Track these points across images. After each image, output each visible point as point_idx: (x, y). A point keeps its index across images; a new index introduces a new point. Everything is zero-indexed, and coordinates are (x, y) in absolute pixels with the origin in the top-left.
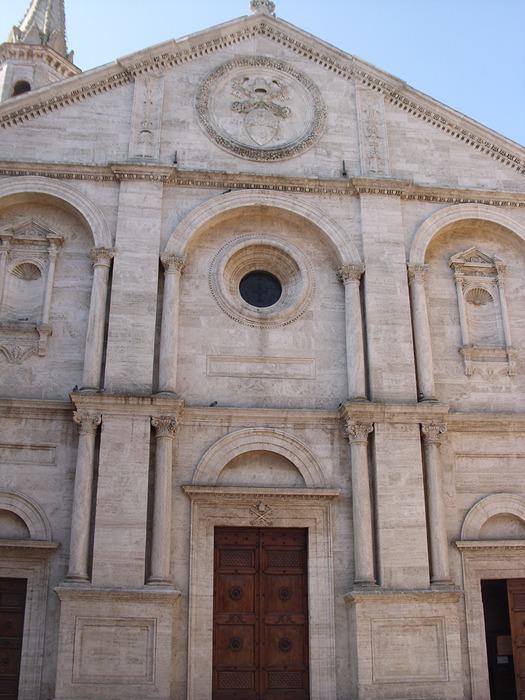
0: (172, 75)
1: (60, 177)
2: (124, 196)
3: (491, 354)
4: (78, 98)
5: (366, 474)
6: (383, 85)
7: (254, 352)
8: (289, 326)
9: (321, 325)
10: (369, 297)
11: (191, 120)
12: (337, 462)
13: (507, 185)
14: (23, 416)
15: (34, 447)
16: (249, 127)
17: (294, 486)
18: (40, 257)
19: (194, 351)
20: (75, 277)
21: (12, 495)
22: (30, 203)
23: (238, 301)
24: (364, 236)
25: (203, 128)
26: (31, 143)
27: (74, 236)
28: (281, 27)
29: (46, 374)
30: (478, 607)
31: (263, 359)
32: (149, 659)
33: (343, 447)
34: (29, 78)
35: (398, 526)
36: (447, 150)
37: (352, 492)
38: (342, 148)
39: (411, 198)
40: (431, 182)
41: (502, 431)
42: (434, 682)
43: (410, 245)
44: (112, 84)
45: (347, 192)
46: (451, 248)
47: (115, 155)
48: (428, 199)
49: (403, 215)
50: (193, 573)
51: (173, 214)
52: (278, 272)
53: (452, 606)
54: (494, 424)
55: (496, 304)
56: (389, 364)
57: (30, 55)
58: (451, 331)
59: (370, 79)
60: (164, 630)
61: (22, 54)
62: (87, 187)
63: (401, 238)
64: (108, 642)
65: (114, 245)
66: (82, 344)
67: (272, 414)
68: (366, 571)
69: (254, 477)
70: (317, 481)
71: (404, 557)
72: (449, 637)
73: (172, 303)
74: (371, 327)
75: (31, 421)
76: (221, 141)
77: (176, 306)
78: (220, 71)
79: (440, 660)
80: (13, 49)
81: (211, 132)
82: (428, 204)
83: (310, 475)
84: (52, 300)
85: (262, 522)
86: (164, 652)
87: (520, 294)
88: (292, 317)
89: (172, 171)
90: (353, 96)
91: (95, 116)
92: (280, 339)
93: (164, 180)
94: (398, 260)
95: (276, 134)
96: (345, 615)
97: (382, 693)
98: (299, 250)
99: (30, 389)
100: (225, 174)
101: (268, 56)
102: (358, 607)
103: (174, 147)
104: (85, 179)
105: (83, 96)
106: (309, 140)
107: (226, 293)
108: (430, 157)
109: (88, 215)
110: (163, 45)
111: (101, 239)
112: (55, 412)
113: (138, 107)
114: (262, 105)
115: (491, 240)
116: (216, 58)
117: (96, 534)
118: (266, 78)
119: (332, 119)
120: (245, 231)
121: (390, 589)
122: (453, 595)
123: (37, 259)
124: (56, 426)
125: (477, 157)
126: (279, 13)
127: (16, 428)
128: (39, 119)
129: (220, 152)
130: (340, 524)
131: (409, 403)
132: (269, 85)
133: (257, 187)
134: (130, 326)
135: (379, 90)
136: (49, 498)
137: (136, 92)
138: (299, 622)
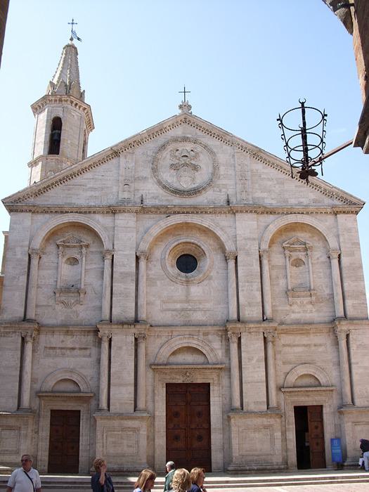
0: (139, 150)
1: (85, 213)
2: (118, 222)
3: (303, 294)
5: (237, 357)
9: (216, 283)
12: (224, 351)
13: (315, 201)
15: (81, 349)
16: (179, 177)
17: (203, 364)
21: (71, 371)
22: (71, 226)
26: (69, 194)
29: (84, 312)
30: (292, 420)
31: (188, 301)
34: (61, 115)
38: (228, 187)
39: (262, 213)
41: (307, 333)
42: (268, 455)
43: (261, 239)
45: (229, 213)
46: (284, 237)
47: (111, 200)
48: (271, 213)
51: (141, 229)
54: (302, 330)
55: (307, 266)
57: (60, 100)
59: (242, 147)
60: (143, 432)
61: (56, 101)
62: (98, 217)
63: (256, 236)
66: (101, 298)
67: (191, 329)
68: (237, 404)
70: (214, 361)
71: (255, 396)
73: (143, 276)
74: (240, 284)
76: (164, 187)
77: (145, 277)
78: (163, 147)
80: (51, 98)
81: (159, 183)
82: (271, 216)
83: (211, 358)
84: (85, 276)
85: (188, 381)
86: (143, 442)
87: (320, 261)
88: (202, 279)
90: (234, 156)
91: (100, 177)
92: (196, 290)
93: (136, 212)
97: (243, 460)
98: (206, 244)
102: (232, 421)
103: (141, 192)
106: (210, 184)
107: (170, 269)
108: (274, 188)
110: (134, 137)
111: (107, 245)
113: (122, 171)
114: (186, 165)
115: (306, 231)
116: (161, 140)
119: (222, 170)
121: (247, 412)
122: (277, 414)
124: (90, 338)
125: (300, 186)
126: (194, 111)
127: (71, 340)
128: (73, 181)
130: (225, 381)
131: (258, 322)
133: (183, 213)
138: (206, 427)
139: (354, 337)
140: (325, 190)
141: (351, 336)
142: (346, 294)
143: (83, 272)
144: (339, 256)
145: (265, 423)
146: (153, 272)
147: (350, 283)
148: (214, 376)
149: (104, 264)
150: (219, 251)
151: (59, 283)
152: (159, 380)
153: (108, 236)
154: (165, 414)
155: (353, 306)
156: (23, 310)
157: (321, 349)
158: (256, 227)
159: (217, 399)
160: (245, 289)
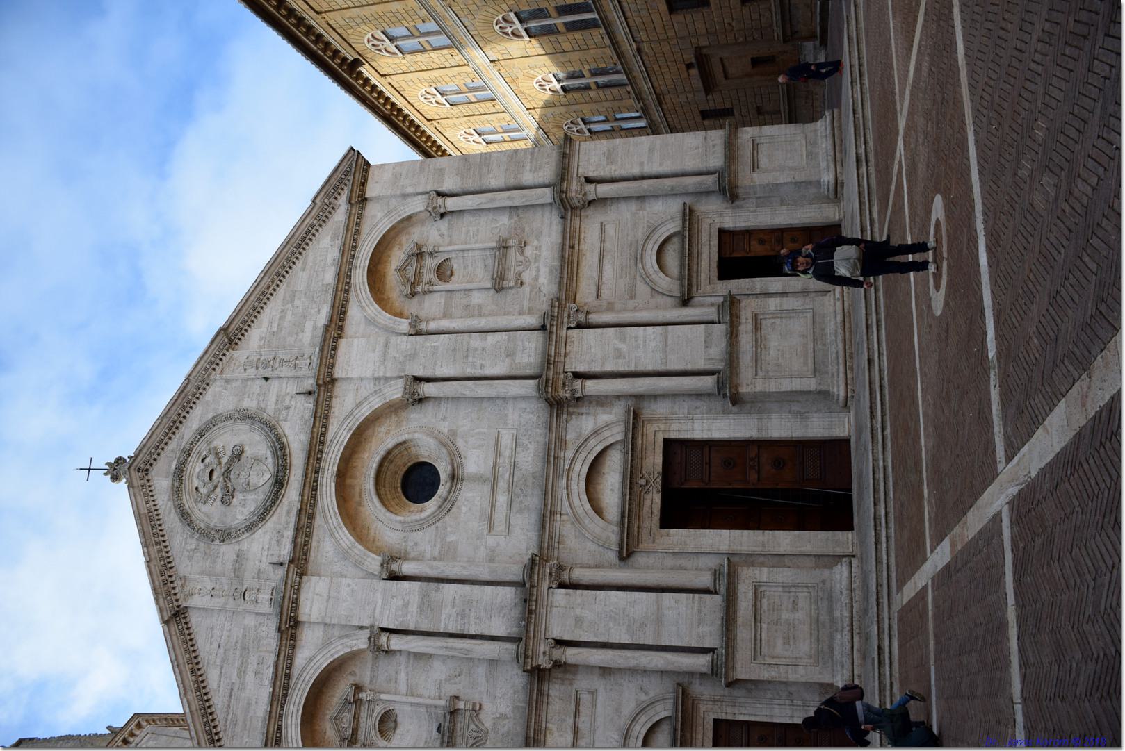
1: (287, 687)
4: (199, 669)
6: (220, 350)
7: (487, 489)
8: (462, 453)
10: (439, 373)
11: (237, 547)
12: (599, 410)
14: (543, 726)
15: (577, 714)
18: (373, 711)
19: (482, 548)
20: (396, 673)
23: (432, 505)
24: (376, 375)
25: (246, 535)
26: (245, 721)
28: (144, 451)
31: (495, 478)
32: (793, 589)
33: (587, 403)
35: (666, 352)
36: (294, 292)
37: (630, 396)
39: (341, 329)
40: (325, 310)
44: (187, 632)
45: (331, 391)
48: (344, 313)
49: (358, 337)
50: (708, 549)
52: (405, 465)
53: (742, 304)
55: (453, 255)
56: (507, 356)
58: (477, 298)
59: (212, 363)
60: (762, 574)
63: (382, 340)
64: (776, 631)
65: (366, 628)
66: (469, 660)
68: (708, 382)
69: (612, 490)
72: (772, 308)
73: (432, 567)
74: (469, 371)
75: (549, 718)
77: (435, 563)
78: (185, 516)
79: (793, 317)
81: (251, 527)
84: (419, 696)
86: (785, 575)
89: (292, 565)
90: (228, 381)
92: (475, 463)
94: (405, 343)
95: (260, 461)
96: (748, 406)
99: (514, 719)
100: (300, 511)
101: (173, 467)
103: (265, 566)
105: (197, 663)
107: (424, 515)
109: (332, 655)
111: (360, 642)
112: (540, 692)
113: (217, 603)
116: (171, 520)
117: (668, 644)
118: (197, 470)
119: (250, 404)
120: (360, 495)
123: (375, 714)
124: (556, 692)
125: (305, 264)
126: (128, 451)
127: (556, 734)
129: (274, 518)
130: (661, 408)
132: (205, 466)
133: (316, 480)
135: (224, 355)
136: (629, 695)
137: (199, 605)
139: (591, 169)
140: (318, 217)
141: (591, 174)
142: (512, 182)
143: (411, 699)
144: (440, 194)
145: (750, 326)
146: (428, 548)
147: (491, 176)
148: (650, 429)
149: (400, 651)
150: (403, 414)
152: (654, 542)
153: (340, 638)
154: (725, 532)
155: (534, 170)
157: (611, 231)
158: (363, 341)
159: (697, 425)
160: (478, 363)
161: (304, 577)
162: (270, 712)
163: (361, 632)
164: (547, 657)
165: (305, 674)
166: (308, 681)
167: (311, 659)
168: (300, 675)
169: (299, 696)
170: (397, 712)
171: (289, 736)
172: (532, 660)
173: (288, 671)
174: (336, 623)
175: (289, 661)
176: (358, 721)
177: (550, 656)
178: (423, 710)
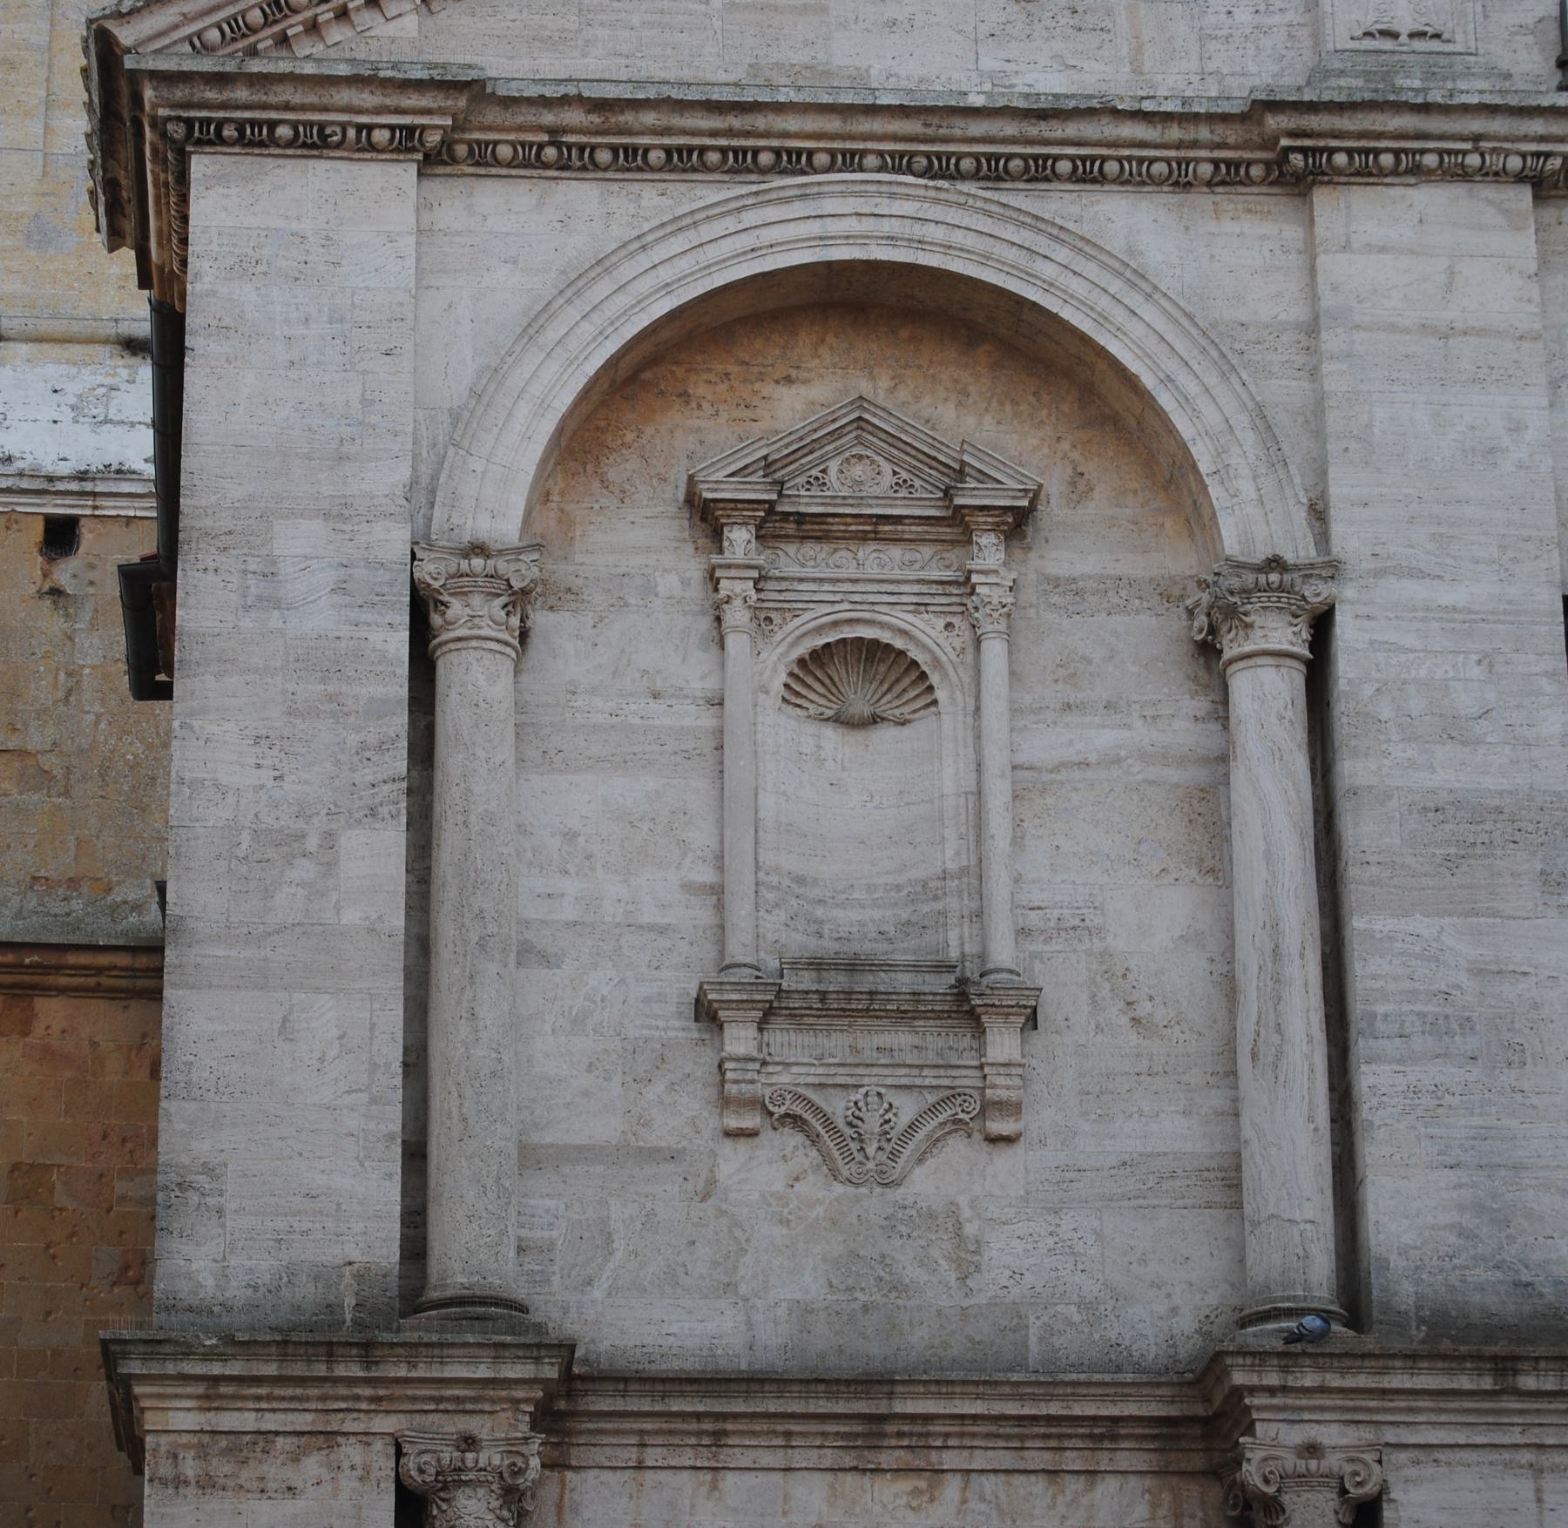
1: (993, 171)
14: (949, 1459)
27: (1079, 487)
65: (1323, 540)
75: (989, 1484)
84: (1018, 841)
104: (1120, 180)
109: (1168, 380)
112: (1107, 1431)
134: (1463, 979)
151: (741, 910)
156: (390, 1195)
161: (1525, 194)
162: (872, 110)
163: (1301, 515)
164: (1290, 1462)
165: (1062, 254)
166: (1030, 277)
167: (1135, 277)
168: (1059, 234)
169: (958, 237)
170: (923, 726)
171: (772, 213)
172: (1271, 1391)
173: (1064, 167)
174: (1329, 385)
175: (1112, 168)
176: (863, 538)
177: (1302, 1478)
178: (952, 854)
